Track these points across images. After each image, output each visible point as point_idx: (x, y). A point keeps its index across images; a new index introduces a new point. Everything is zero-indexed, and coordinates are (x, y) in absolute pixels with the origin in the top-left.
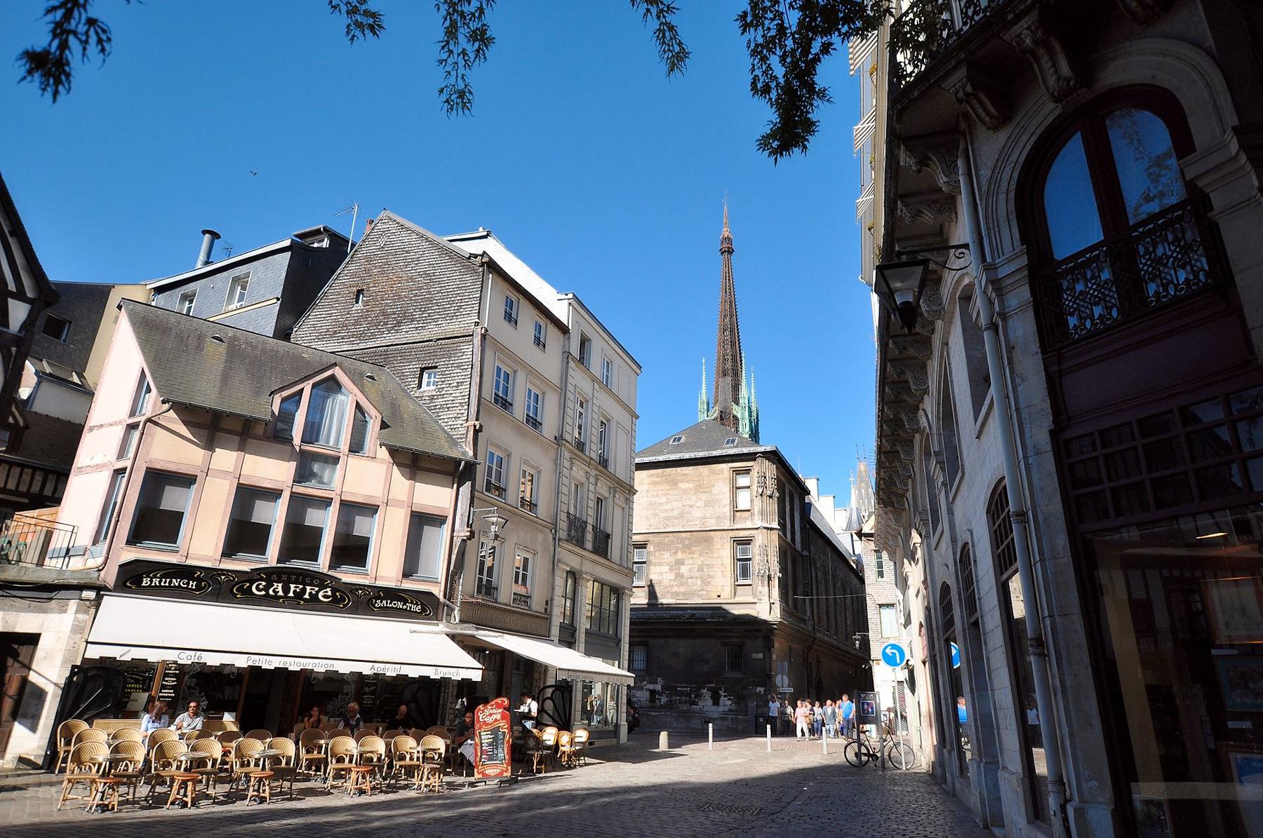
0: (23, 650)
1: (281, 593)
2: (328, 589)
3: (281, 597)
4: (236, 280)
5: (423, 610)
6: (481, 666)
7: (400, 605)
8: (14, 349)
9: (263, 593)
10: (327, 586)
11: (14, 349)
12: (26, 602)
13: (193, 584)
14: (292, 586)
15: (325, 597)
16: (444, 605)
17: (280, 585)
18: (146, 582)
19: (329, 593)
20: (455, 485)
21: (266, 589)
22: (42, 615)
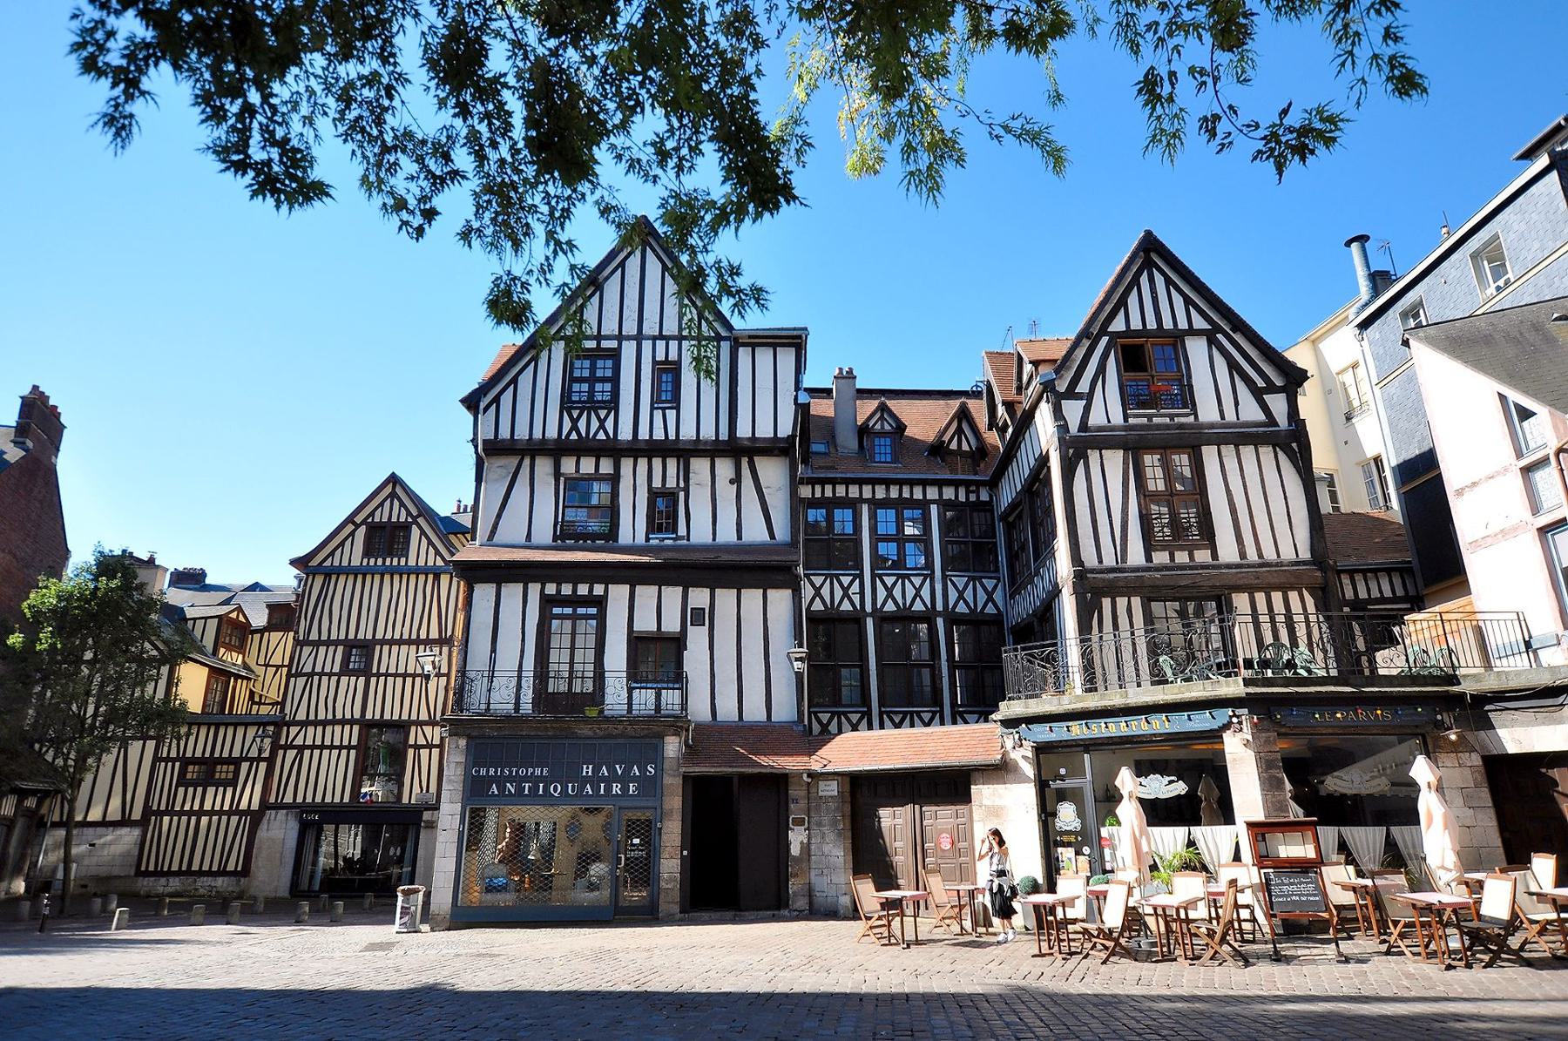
4: (1475, 257)
8: (1294, 445)
11: (1294, 445)
12: (1530, 715)
22: (1559, 727)
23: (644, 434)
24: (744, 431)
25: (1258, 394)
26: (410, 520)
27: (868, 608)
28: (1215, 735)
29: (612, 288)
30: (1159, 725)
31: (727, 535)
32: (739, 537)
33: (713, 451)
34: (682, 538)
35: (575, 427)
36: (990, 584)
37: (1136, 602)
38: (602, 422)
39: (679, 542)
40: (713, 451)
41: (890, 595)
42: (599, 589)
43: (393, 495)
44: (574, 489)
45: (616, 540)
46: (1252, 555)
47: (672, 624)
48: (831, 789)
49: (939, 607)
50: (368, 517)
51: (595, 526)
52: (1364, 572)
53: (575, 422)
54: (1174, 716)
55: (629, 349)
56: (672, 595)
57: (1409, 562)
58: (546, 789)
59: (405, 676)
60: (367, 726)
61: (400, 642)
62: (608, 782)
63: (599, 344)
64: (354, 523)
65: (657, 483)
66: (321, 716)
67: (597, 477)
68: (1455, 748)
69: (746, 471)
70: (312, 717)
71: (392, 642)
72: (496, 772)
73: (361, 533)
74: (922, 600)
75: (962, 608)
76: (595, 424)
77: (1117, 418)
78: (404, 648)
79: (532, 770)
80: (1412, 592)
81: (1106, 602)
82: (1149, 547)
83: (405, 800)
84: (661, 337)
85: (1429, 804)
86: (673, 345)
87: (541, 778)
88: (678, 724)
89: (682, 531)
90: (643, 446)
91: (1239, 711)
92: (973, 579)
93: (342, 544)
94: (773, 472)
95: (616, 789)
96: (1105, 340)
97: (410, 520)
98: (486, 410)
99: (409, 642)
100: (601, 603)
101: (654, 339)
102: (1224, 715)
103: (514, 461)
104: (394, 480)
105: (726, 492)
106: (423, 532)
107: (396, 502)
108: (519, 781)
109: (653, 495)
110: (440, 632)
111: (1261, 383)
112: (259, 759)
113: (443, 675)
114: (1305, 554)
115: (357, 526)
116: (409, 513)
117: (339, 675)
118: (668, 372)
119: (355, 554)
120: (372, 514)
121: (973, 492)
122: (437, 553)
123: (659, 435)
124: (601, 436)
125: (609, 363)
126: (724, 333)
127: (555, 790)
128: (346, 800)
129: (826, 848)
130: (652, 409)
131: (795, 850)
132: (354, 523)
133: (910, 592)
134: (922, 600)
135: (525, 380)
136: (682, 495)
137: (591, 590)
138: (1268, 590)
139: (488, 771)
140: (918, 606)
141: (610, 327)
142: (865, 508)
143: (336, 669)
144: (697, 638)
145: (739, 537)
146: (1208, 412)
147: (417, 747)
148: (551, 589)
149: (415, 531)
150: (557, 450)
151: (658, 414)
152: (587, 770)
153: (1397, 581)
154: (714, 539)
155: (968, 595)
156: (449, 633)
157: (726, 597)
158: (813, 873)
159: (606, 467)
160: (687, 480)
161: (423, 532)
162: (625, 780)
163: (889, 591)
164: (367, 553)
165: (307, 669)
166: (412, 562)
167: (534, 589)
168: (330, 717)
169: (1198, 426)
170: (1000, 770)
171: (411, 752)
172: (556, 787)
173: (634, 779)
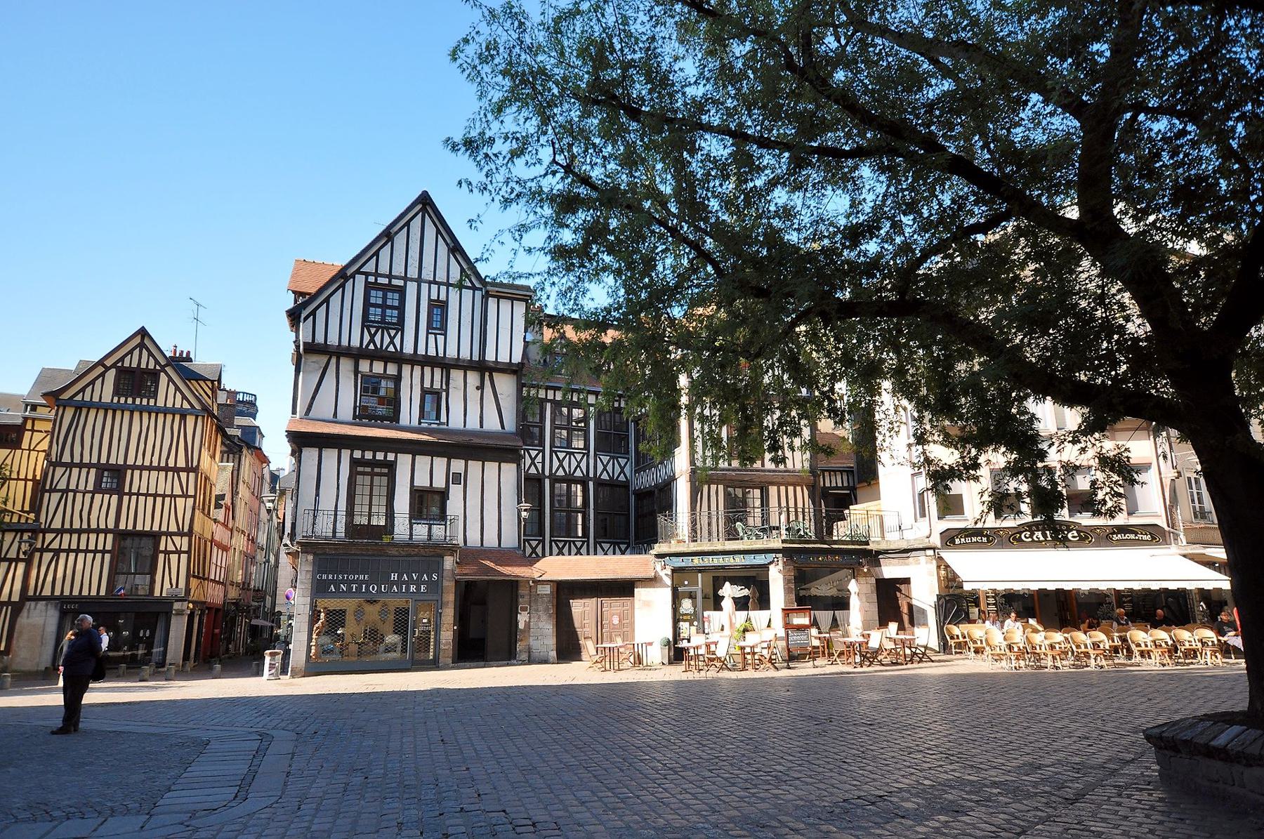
0: (902, 587)
1: (1042, 539)
2: (1074, 532)
3: (1043, 541)
5: (1153, 538)
6: (1228, 578)
7: (1132, 536)
9: (1030, 540)
10: (1072, 530)
13: (985, 539)
14: (1048, 532)
15: (1073, 537)
16: (1169, 532)
17: (1040, 533)
18: (957, 541)
19: (1076, 534)
20: (1152, 437)
21: (1031, 536)
23: (421, 351)
24: (490, 356)
26: (158, 367)
27: (547, 473)
28: (765, 567)
29: (400, 240)
30: (739, 560)
31: (473, 424)
32: (482, 426)
33: (467, 366)
34: (443, 424)
35: (372, 341)
36: (623, 461)
37: (721, 487)
38: (392, 339)
39: (441, 427)
40: (467, 366)
41: (561, 465)
42: (391, 457)
43: (141, 346)
44: (369, 385)
45: (398, 421)
47: (439, 483)
48: (546, 590)
49: (591, 475)
50: (118, 362)
51: (382, 410)
52: (830, 471)
53: (372, 336)
54: (747, 556)
55: (411, 288)
56: (440, 463)
57: (852, 467)
58: (367, 588)
59: (155, 496)
60: (121, 536)
61: (150, 468)
62: (408, 584)
63: (390, 281)
64: (104, 366)
65: (427, 384)
66: (76, 525)
67: (384, 376)
68: (865, 575)
69: (487, 382)
70: (67, 526)
71: (142, 468)
72: (333, 577)
73: (111, 374)
74: (581, 470)
75: (605, 476)
76: (387, 340)
78: (154, 474)
79: (356, 576)
80: (851, 484)
81: (706, 488)
83: (157, 593)
84: (435, 282)
85: (855, 602)
86: (443, 289)
87: (363, 582)
88: (452, 549)
89: (443, 419)
90: (421, 359)
91: (778, 555)
92: (613, 458)
93: (93, 382)
94: (506, 385)
95: (413, 588)
97: (158, 367)
98: (305, 319)
99: (159, 469)
100: (391, 467)
101: (430, 283)
102: (771, 557)
103: (324, 359)
104: (143, 332)
105: (473, 395)
106: (170, 379)
107: (145, 353)
108: (349, 582)
109: (424, 392)
112: (17, 560)
113: (191, 496)
115: (107, 369)
116: (157, 362)
117: (93, 493)
118: (440, 307)
119: (106, 392)
120: (122, 359)
121: (617, 401)
122: (184, 397)
123: (432, 352)
124: (391, 349)
125: (396, 296)
126: (478, 285)
127: (373, 588)
128: (103, 593)
129: (541, 625)
130: (428, 333)
131: (521, 626)
132: (104, 366)
133: (574, 464)
134: (581, 470)
135: (335, 301)
136: (444, 394)
137: (385, 457)
138: (787, 485)
139: (328, 577)
140: (578, 474)
141: (398, 270)
142: (549, 405)
143: (90, 487)
144: (456, 491)
145: (482, 426)
147: (167, 552)
148: (358, 454)
149: (163, 379)
150: (357, 355)
151: (432, 337)
152: (394, 577)
153: (845, 478)
154: (465, 426)
155: (609, 468)
156: (195, 464)
157: (474, 466)
158: (531, 639)
159: (392, 369)
160: (448, 384)
161: (170, 379)
162: (418, 583)
163: (561, 462)
164: (117, 392)
165: (62, 486)
166: (160, 403)
167: (346, 454)
168: (85, 526)
170: (652, 581)
171: (161, 556)
172: (373, 587)
173: (424, 582)
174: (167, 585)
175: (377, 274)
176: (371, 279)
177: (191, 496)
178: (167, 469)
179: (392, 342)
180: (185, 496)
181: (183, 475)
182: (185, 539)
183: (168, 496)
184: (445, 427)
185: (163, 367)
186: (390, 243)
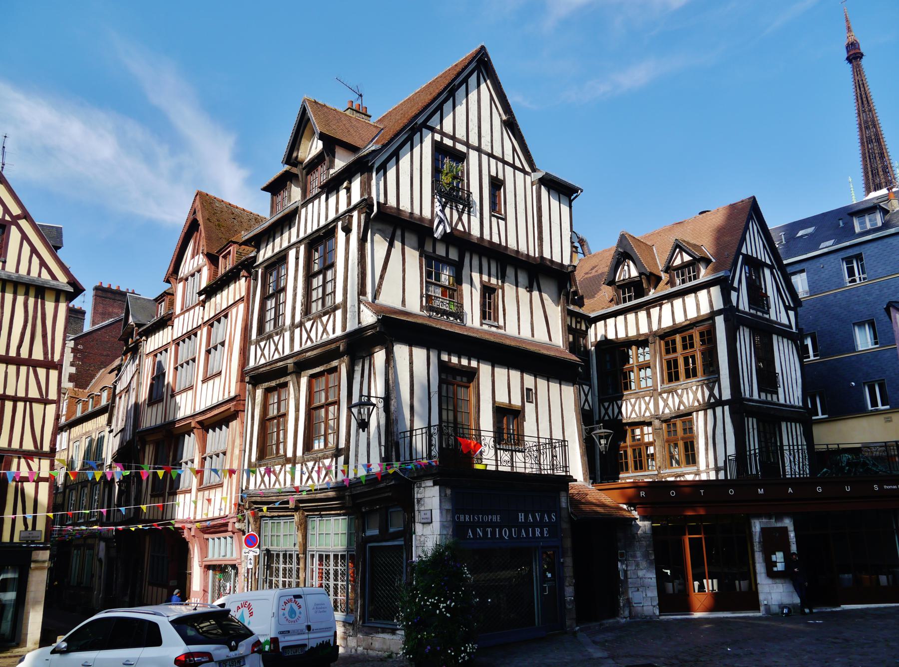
25: (787, 308)
26: (7, 218)
31: (526, 334)
32: (533, 335)
37: (755, 420)
42: (474, 364)
46: (788, 402)
77: (747, 310)
79: (490, 517)
82: (760, 390)
89: (501, 323)
96: (741, 256)
97: (7, 218)
106: (24, 237)
110: (45, 353)
111: (787, 304)
113: (52, 402)
114: (801, 404)
118: (497, 184)
122: (43, 264)
129: (641, 573)
130: (491, 216)
136: (500, 291)
145: (533, 335)
146: (773, 317)
148: (445, 357)
149: (14, 235)
152: (521, 517)
156: (57, 358)
158: (630, 591)
161: (24, 237)
166: (10, 267)
169: (769, 320)
174: (20, 526)
175: (443, 134)
176: (438, 137)
177: (52, 402)
178: (18, 362)
179: (460, 219)
180: (45, 401)
181: (42, 372)
182: (46, 463)
183: (21, 399)
184: (502, 331)
185: (15, 220)
186: (451, 99)
